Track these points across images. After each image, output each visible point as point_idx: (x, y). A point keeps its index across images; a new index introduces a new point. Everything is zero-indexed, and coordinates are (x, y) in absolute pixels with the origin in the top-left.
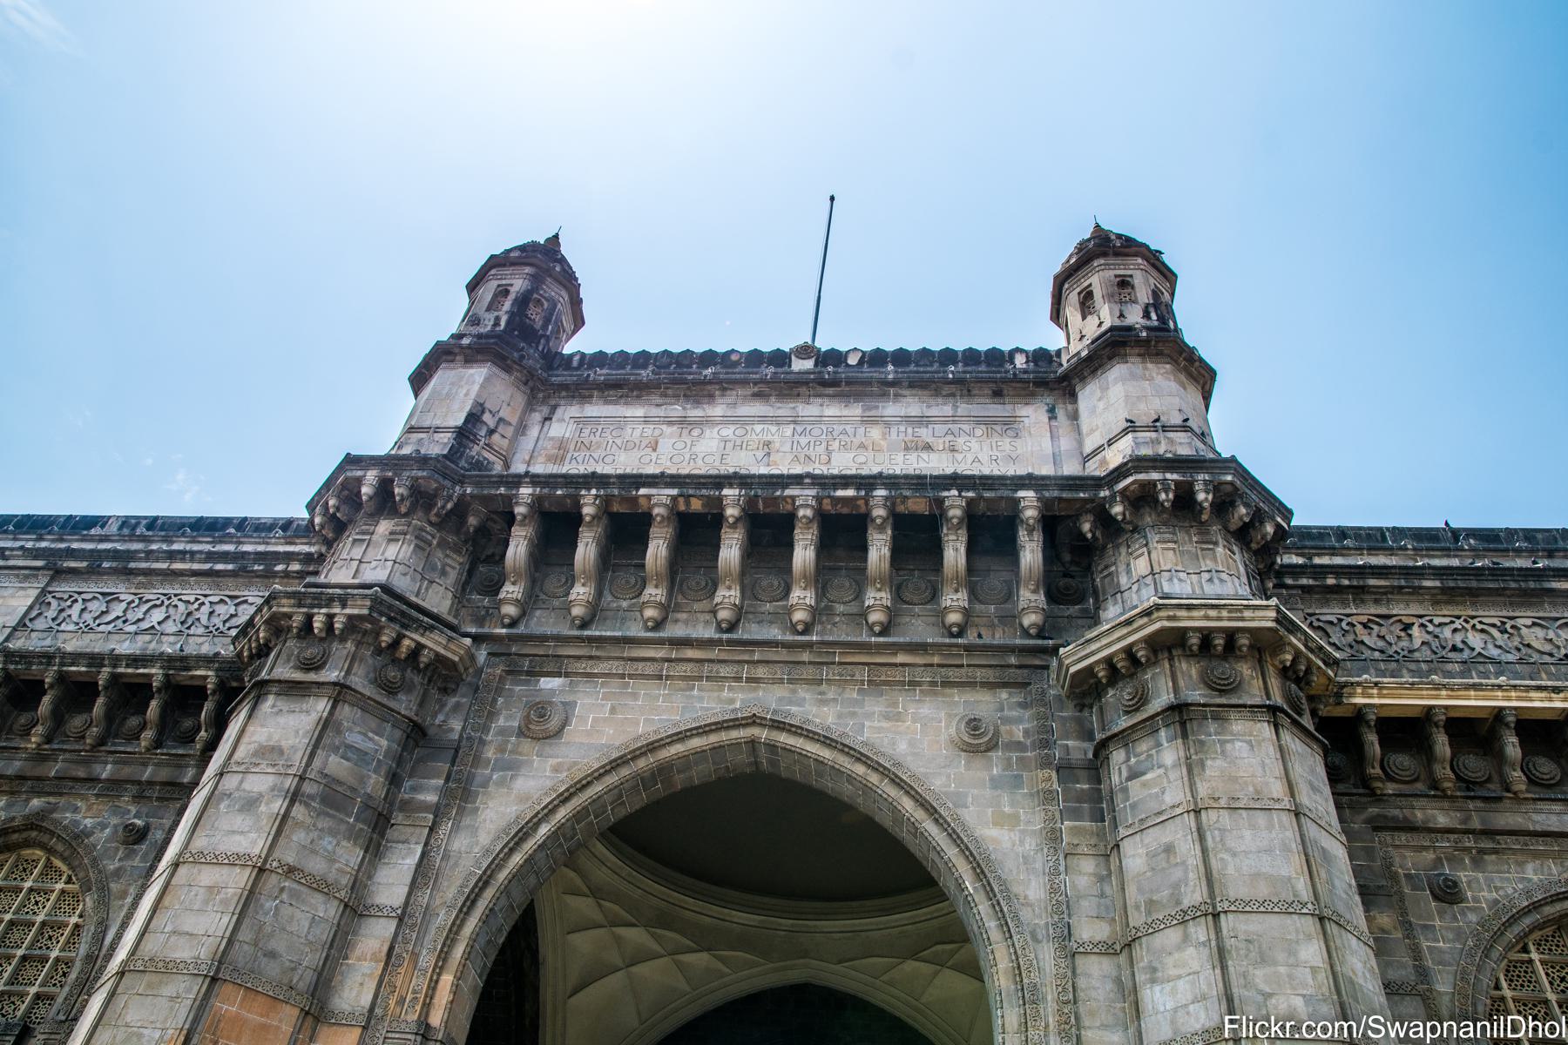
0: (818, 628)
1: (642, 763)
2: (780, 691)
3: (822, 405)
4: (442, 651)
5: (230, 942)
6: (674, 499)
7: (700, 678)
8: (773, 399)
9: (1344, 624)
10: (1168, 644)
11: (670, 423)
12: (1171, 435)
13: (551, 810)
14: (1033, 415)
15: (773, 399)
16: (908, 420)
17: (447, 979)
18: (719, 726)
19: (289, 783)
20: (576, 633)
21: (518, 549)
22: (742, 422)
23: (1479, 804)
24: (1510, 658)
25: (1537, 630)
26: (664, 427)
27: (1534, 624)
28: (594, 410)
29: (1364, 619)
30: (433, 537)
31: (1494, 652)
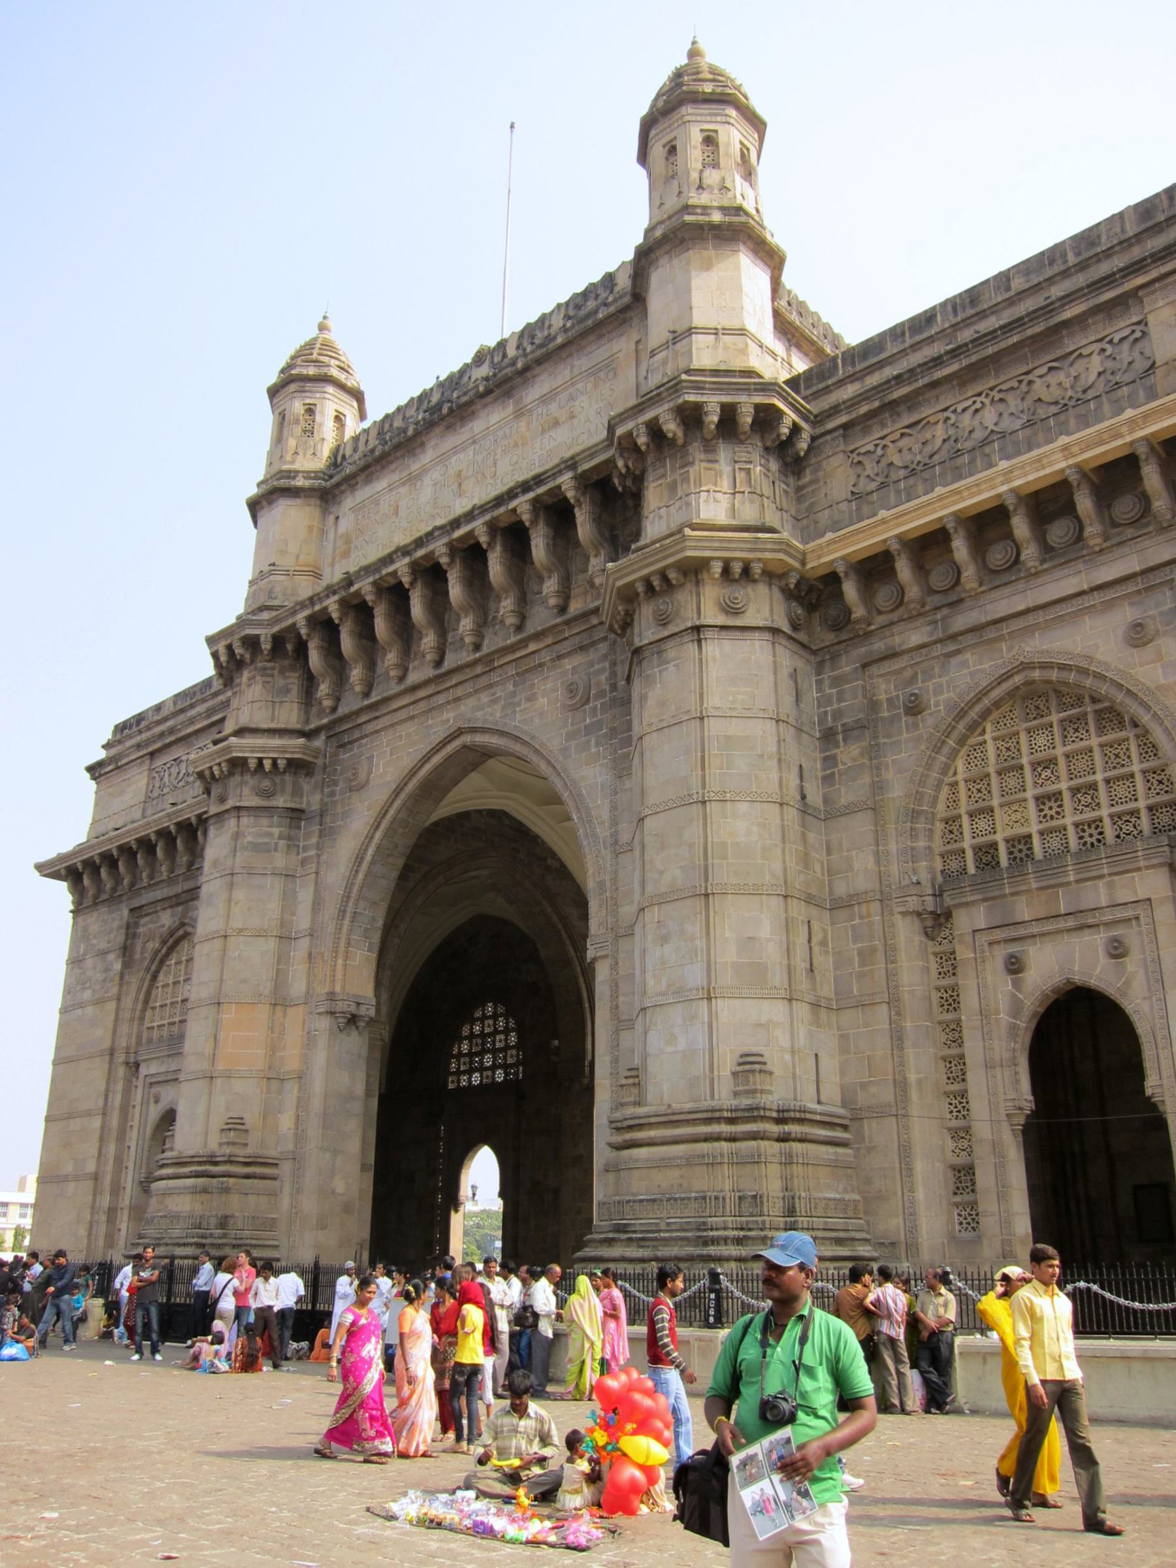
0: (486, 642)
2: (471, 702)
4: (288, 756)
5: (221, 981)
6: (375, 583)
7: (430, 710)
9: (879, 452)
11: (403, 484)
12: (678, 346)
14: (621, 346)
16: (545, 400)
17: (340, 961)
21: (315, 658)
22: (443, 459)
23: (945, 611)
25: (1052, 379)
27: (1050, 369)
28: (363, 493)
30: (273, 668)
31: (1007, 424)
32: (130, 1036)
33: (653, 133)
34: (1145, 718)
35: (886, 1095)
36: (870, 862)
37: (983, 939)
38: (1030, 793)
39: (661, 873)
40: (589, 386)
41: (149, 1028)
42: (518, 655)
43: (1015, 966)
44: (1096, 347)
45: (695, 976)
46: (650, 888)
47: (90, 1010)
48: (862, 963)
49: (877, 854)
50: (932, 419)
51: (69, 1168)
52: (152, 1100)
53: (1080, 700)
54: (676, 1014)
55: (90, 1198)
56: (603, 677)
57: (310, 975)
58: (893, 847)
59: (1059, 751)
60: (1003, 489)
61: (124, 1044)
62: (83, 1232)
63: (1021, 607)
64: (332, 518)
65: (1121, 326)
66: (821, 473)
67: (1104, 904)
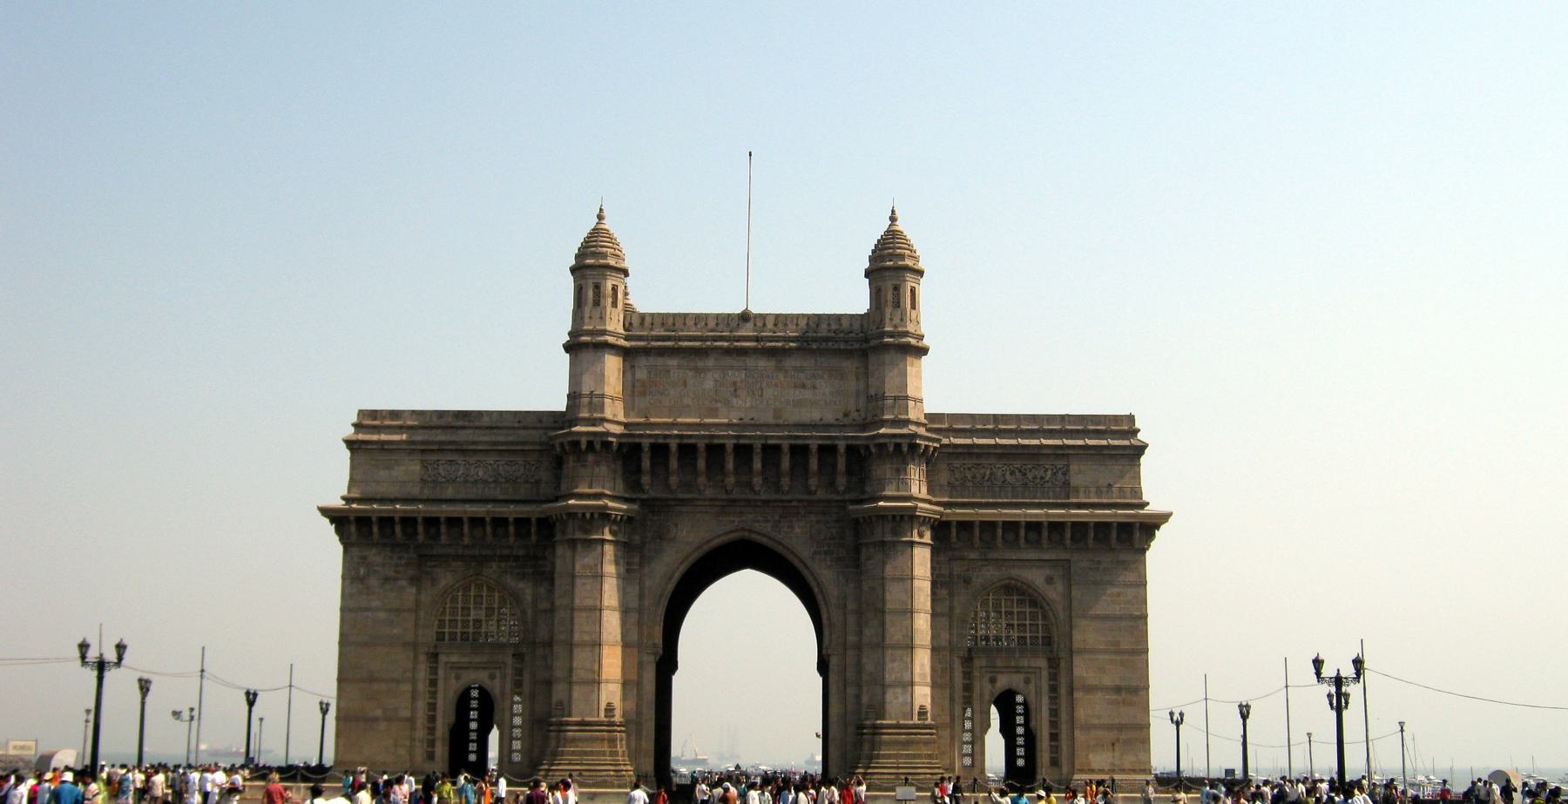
1: (706, 548)
2: (751, 517)
3: (757, 358)
8: (735, 355)
10: (883, 517)
11: (690, 370)
13: (678, 568)
14: (850, 365)
15: (735, 355)
16: (796, 369)
18: (731, 532)
20: (673, 497)
21: (646, 463)
26: (687, 371)
27: (1034, 467)
28: (652, 360)
29: (969, 466)
33: (887, 274)
34: (1047, 608)
37: (984, 670)
40: (826, 376)
41: (437, 632)
42: (785, 504)
43: (993, 681)
44: (1051, 467)
45: (907, 677)
46: (888, 641)
47: (382, 615)
48: (942, 672)
50: (986, 466)
51: (379, 713)
52: (453, 675)
53: (1023, 594)
54: (899, 690)
56: (834, 531)
57: (640, 634)
59: (1015, 610)
60: (1022, 519)
62: (402, 752)
63: (1014, 558)
65: (1060, 463)
67: (1026, 665)
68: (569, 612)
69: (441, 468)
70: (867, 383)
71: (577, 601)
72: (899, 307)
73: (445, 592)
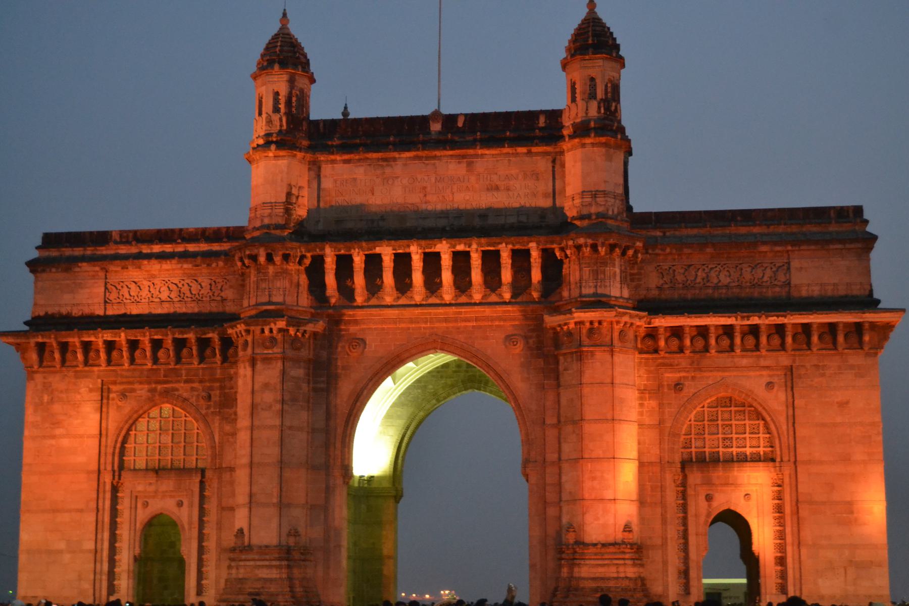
4: (313, 330)
9: (671, 271)
19: (279, 398)
24: (734, 284)
27: (750, 266)
28: (340, 167)
32: (113, 463)
34: (768, 419)
35: (659, 542)
36: (658, 453)
38: (720, 436)
39: (592, 451)
40: (520, 177)
43: (709, 498)
49: (660, 449)
51: (62, 545)
55: (92, 565)
58: (666, 447)
61: (109, 468)
62: (87, 586)
64: (313, 173)
66: (643, 271)
68: (249, 433)
69: (125, 290)
70: (564, 183)
71: (256, 423)
72: (595, 98)
73: (130, 418)
